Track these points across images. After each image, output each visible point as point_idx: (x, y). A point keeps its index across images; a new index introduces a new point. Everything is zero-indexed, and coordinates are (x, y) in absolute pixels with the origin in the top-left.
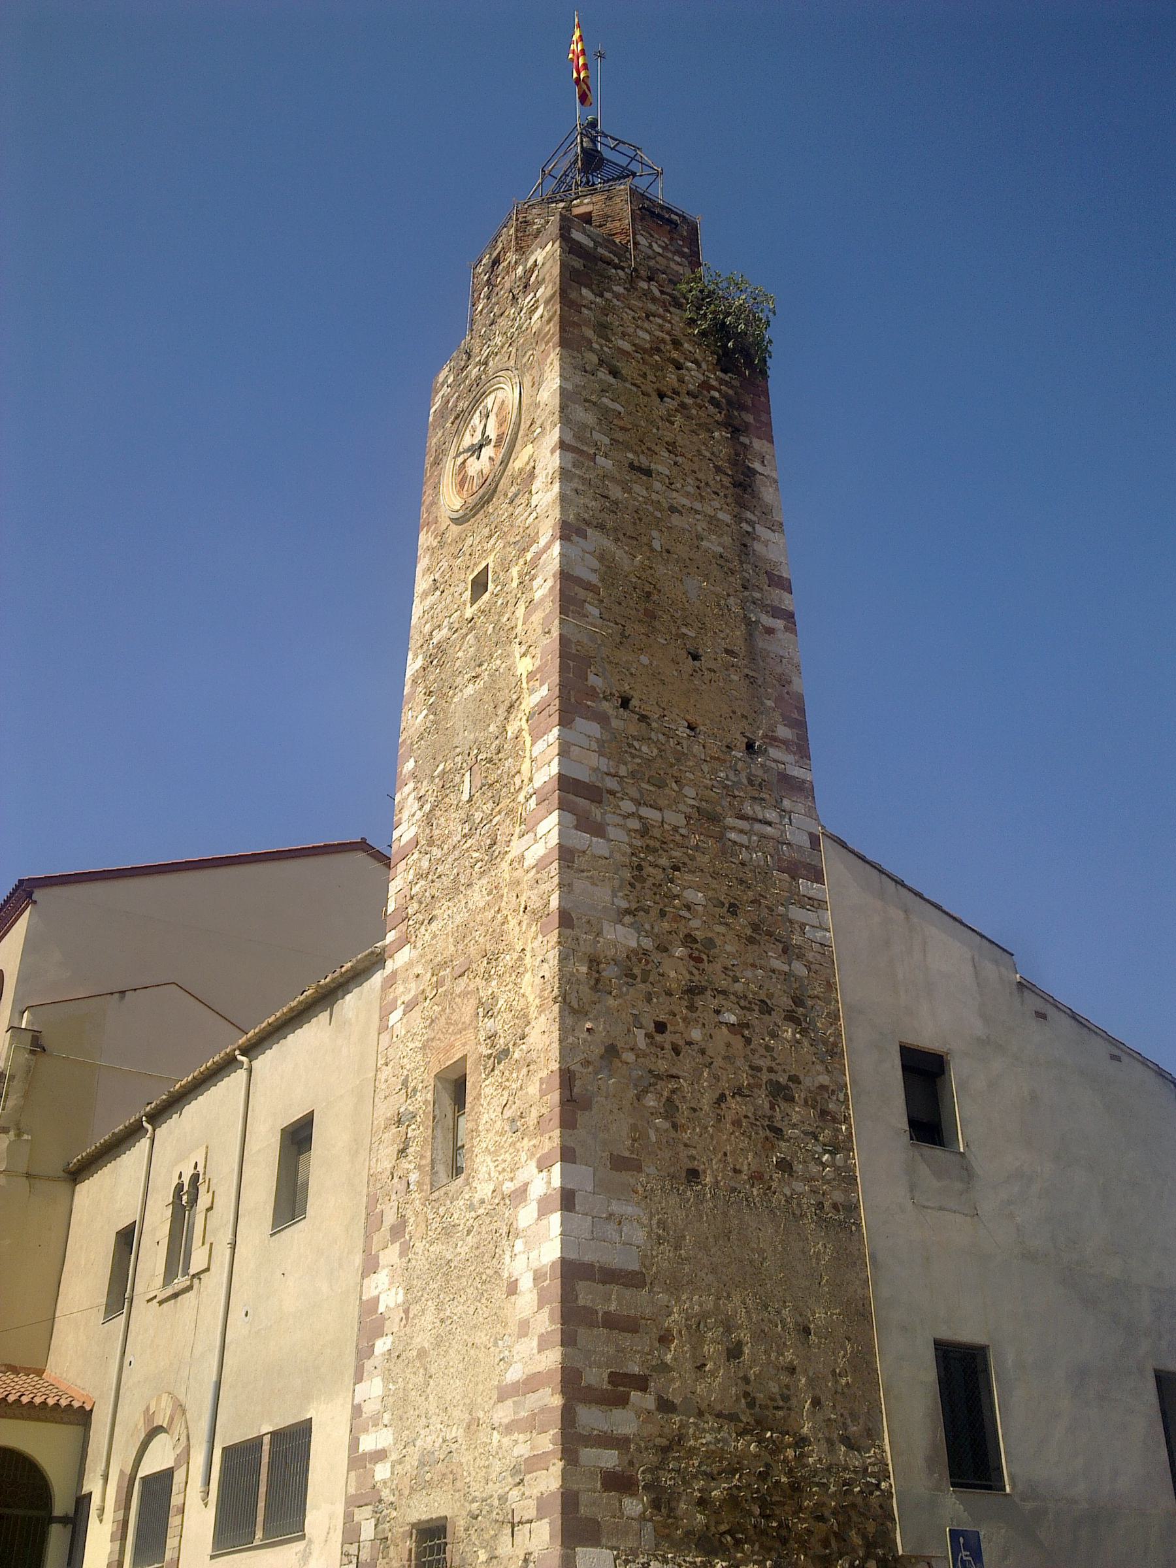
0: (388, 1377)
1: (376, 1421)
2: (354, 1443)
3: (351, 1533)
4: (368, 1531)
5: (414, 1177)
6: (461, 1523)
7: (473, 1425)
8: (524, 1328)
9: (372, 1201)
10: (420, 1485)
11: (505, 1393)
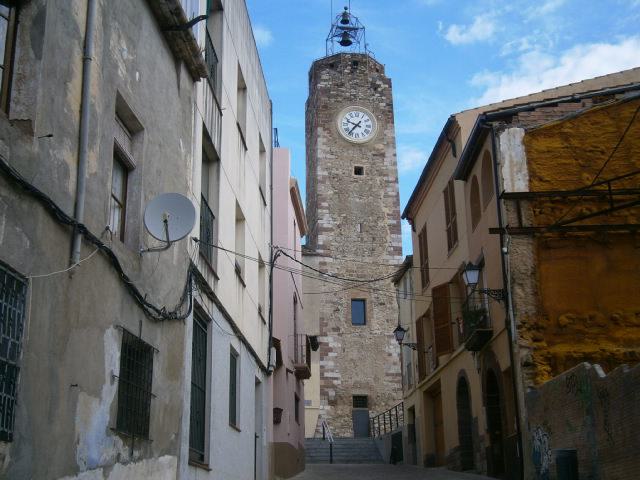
0: (336, 362)
1: (332, 371)
2: (322, 374)
3: (323, 393)
4: (332, 393)
5: (342, 319)
6: (374, 397)
7: (376, 379)
8: (395, 364)
9: (322, 319)
10: (355, 386)
11: (388, 375)
